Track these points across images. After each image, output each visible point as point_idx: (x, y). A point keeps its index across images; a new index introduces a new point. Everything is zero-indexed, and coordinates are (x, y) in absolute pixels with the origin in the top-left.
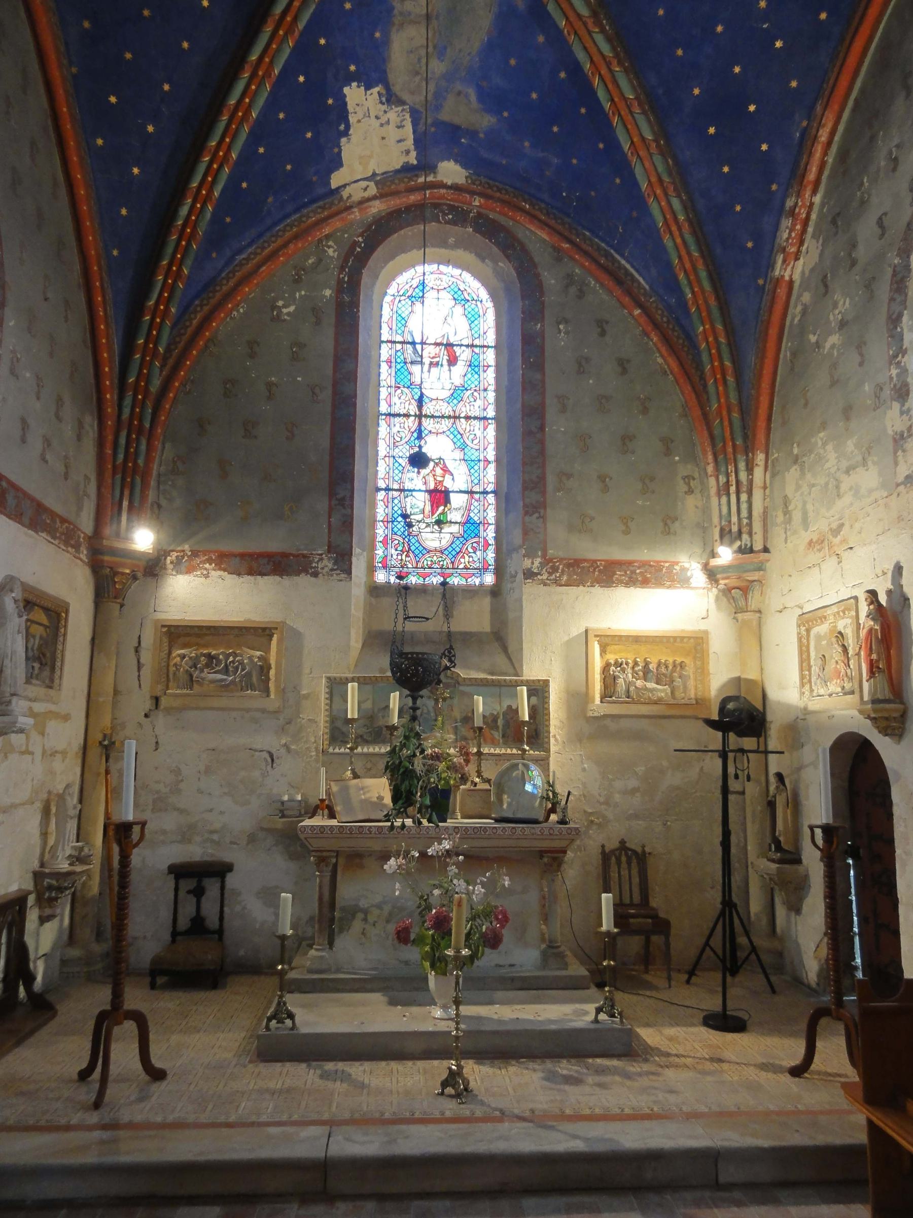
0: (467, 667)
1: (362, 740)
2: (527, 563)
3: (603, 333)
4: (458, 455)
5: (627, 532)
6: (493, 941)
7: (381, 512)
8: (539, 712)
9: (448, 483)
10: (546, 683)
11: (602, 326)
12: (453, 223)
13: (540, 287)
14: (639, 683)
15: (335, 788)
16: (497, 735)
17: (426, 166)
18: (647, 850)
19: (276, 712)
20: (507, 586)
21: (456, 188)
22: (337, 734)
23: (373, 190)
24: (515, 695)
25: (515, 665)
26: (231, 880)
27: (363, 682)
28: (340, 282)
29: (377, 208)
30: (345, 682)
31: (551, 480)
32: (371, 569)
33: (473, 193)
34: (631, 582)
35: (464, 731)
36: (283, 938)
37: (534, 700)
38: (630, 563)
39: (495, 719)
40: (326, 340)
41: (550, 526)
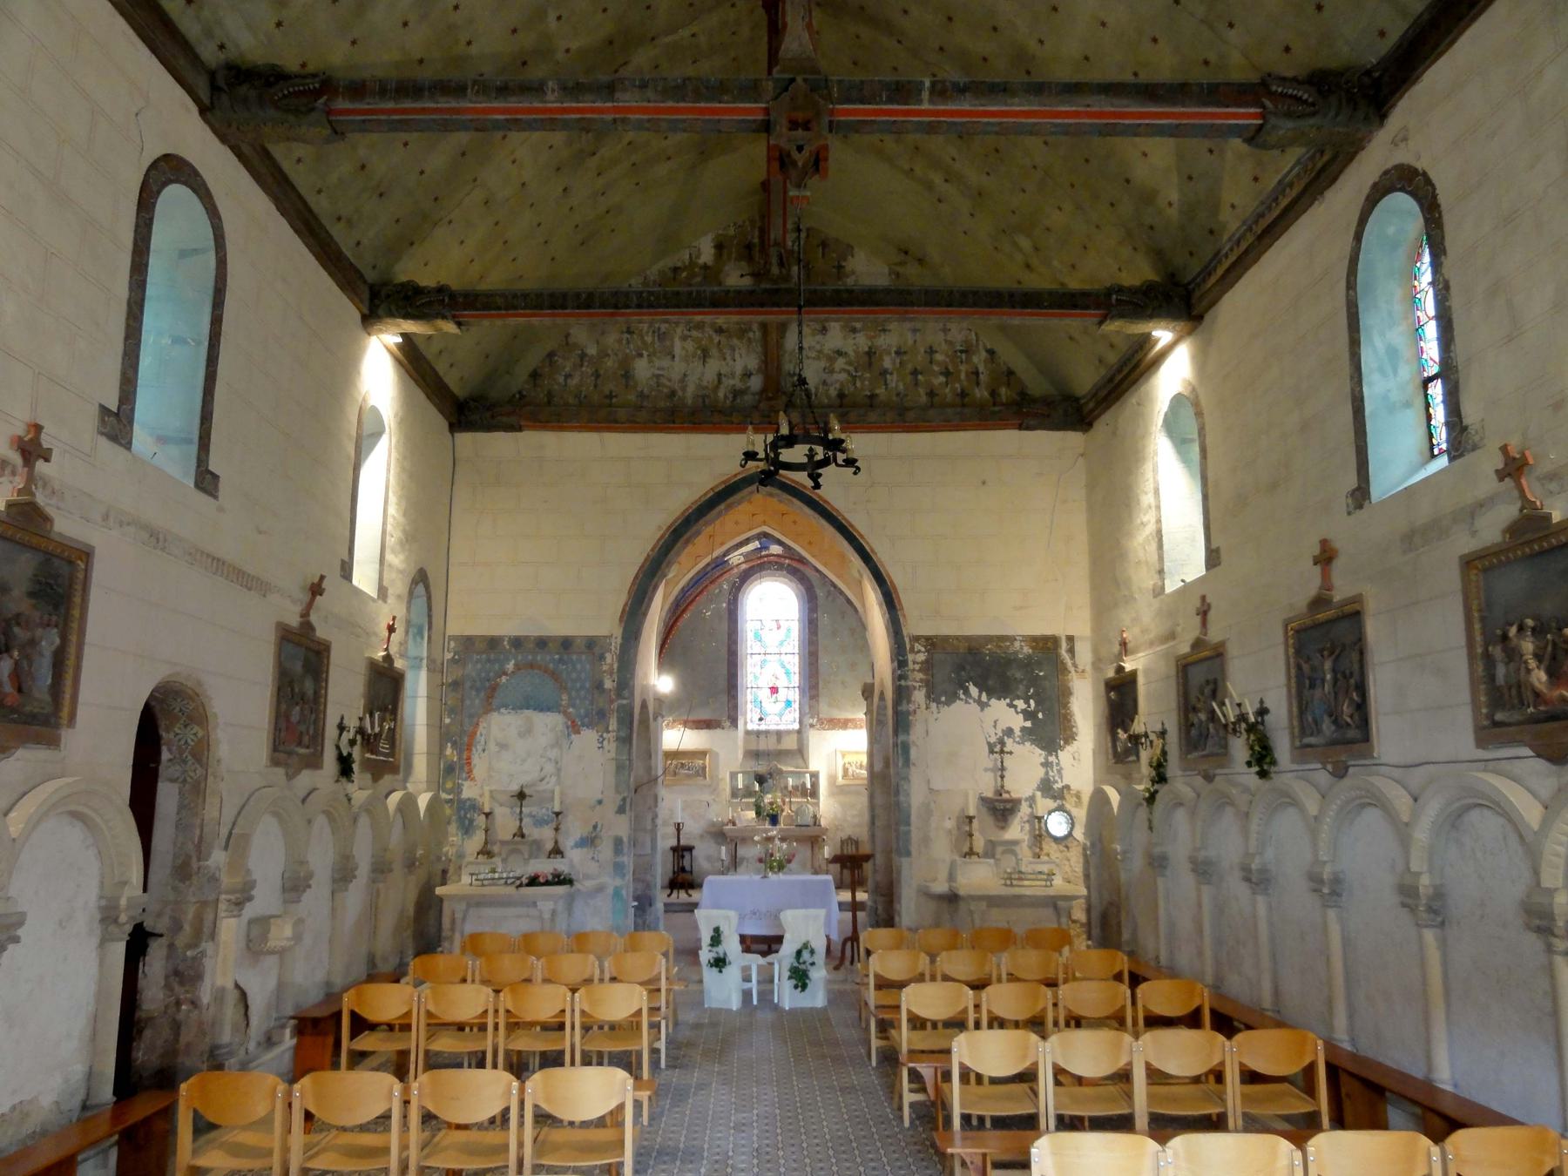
0: (786, 765)
3: (843, 617)
4: (783, 671)
6: (789, 861)
7: (749, 697)
8: (815, 785)
9: (778, 684)
10: (818, 772)
12: (777, 570)
14: (858, 771)
16: (799, 793)
17: (764, 548)
19: (710, 786)
21: (778, 556)
22: (735, 793)
23: (742, 559)
26: (694, 852)
27: (743, 773)
29: (744, 566)
30: (737, 773)
32: (746, 723)
33: (785, 558)
34: (855, 727)
35: (785, 792)
36: (723, 860)
38: (854, 720)
40: (725, 626)
41: (821, 705)
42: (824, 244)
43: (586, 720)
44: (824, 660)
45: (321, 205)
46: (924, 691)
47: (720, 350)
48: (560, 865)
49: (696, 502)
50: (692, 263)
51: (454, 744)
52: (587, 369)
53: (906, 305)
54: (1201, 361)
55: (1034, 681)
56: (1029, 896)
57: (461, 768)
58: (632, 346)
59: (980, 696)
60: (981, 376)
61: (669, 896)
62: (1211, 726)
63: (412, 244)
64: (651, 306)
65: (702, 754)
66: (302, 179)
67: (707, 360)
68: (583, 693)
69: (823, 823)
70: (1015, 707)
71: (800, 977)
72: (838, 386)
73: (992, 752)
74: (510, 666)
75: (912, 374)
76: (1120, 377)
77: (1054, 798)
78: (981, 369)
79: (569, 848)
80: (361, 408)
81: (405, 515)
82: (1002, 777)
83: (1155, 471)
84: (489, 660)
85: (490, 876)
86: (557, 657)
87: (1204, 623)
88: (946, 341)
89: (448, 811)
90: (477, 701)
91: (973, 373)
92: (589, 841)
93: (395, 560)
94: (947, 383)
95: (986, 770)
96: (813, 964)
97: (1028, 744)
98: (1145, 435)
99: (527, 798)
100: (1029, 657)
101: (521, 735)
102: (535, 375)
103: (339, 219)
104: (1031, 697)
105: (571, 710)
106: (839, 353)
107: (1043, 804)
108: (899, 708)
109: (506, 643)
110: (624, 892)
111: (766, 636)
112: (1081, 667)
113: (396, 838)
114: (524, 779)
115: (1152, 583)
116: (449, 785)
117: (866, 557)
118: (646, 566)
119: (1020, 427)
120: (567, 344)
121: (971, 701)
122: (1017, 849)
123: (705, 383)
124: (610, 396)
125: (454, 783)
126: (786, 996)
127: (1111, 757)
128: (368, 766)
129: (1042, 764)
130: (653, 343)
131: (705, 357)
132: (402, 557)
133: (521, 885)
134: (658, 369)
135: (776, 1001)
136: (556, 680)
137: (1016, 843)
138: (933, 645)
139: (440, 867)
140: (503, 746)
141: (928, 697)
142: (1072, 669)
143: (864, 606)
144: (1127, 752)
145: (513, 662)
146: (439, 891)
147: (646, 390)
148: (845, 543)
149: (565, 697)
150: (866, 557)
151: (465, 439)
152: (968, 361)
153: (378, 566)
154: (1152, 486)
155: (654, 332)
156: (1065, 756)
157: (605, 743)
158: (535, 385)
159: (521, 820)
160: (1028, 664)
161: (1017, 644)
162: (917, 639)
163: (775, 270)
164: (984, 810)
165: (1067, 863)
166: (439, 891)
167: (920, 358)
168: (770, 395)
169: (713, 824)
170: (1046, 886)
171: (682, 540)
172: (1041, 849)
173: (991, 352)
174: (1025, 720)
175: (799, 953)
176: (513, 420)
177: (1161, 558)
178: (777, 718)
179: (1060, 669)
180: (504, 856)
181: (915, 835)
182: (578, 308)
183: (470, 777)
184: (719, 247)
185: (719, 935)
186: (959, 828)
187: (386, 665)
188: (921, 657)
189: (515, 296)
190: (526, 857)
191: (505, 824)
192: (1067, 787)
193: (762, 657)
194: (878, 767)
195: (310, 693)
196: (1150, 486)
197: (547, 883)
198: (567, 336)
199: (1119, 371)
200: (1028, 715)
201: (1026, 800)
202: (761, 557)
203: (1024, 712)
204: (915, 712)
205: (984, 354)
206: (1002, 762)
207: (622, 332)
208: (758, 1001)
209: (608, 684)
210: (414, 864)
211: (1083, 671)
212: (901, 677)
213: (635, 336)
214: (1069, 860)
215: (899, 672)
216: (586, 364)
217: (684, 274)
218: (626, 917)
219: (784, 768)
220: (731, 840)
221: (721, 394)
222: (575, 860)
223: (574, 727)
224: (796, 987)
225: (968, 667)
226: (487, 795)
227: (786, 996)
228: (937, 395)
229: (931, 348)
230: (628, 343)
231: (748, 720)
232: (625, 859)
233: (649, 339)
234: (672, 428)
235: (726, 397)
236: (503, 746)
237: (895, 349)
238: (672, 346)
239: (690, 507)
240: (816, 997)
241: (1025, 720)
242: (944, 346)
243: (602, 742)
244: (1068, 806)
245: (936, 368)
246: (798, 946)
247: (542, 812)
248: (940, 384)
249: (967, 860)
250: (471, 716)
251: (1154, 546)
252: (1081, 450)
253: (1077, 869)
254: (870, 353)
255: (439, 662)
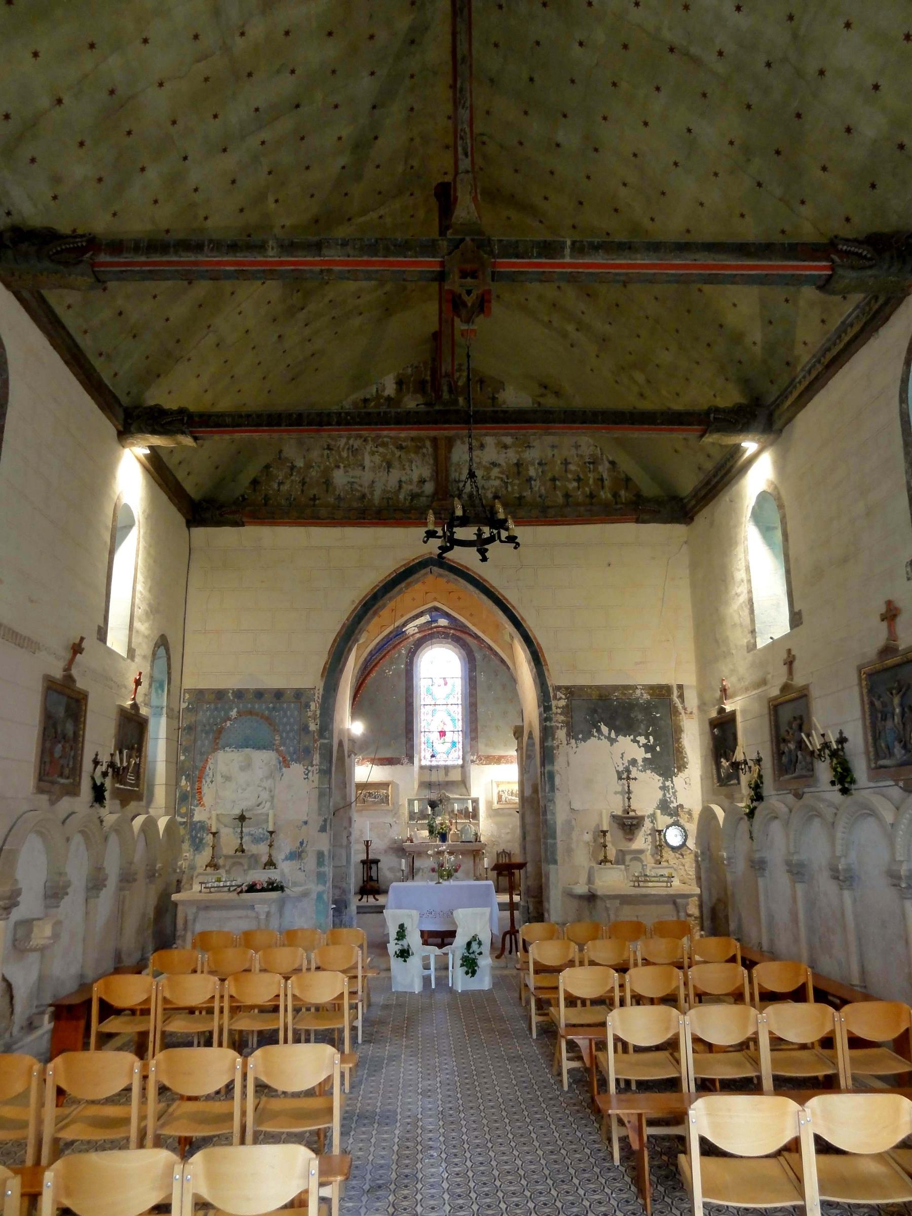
0: (452, 793)
1: (419, 819)
2: (472, 758)
5: (505, 745)
6: (456, 871)
7: (423, 739)
9: (446, 729)
11: (496, 673)
12: (444, 638)
13: (475, 659)
14: (510, 797)
15: (412, 833)
16: (463, 816)
17: (434, 621)
18: (512, 853)
20: (466, 765)
21: (445, 627)
22: (412, 816)
23: (417, 630)
24: (467, 803)
25: (469, 794)
27: (419, 800)
28: (407, 662)
29: (418, 636)
31: (479, 728)
32: (420, 760)
33: (451, 628)
34: (507, 762)
36: (403, 871)
37: (474, 804)
38: (507, 756)
39: (462, 810)
40: (403, 684)
41: (479, 744)
42: (481, 381)
43: (295, 756)
44: (481, 709)
45: (86, 343)
46: (565, 730)
47: (401, 462)
48: (273, 875)
49: (382, 581)
50: (378, 396)
51: (188, 777)
52: (296, 478)
53: (550, 422)
54: (781, 466)
55: (653, 721)
56: (654, 895)
57: (193, 797)
58: (331, 460)
59: (610, 734)
60: (606, 483)
61: (360, 900)
62: (799, 753)
63: (159, 376)
64: (348, 424)
65: (385, 785)
66: (70, 320)
67: (391, 470)
68: (291, 735)
69: (483, 839)
70: (638, 742)
71: (470, 965)
72: (493, 490)
73: (620, 778)
74: (234, 713)
75: (550, 480)
76: (716, 480)
77: (671, 815)
78: (605, 476)
79: (280, 861)
80: (116, 505)
81: (150, 591)
82: (629, 799)
83: (746, 552)
84: (216, 709)
85: (216, 884)
86: (271, 705)
87: (790, 672)
88: (577, 455)
89: (182, 831)
90: (207, 742)
91: (598, 479)
92: (296, 855)
93: (142, 627)
94: (579, 488)
95: (616, 793)
96: (480, 953)
97: (649, 772)
98: (737, 524)
99: (247, 820)
100: (648, 702)
101: (242, 769)
102: (255, 482)
103: (101, 355)
104: (650, 734)
105: (282, 748)
106: (494, 464)
107: (663, 820)
108: (546, 744)
109: (230, 694)
110: (325, 897)
111: (435, 689)
112: (689, 710)
113: (139, 855)
114: (244, 805)
115: (746, 641)
116: (183, 810)
117: (517, 623)
118: (343, 632)
119: (637, 521)
120: (280, 458)
121: (603, 738)
122: (642, 857)
123: (389, 488)
124: (314, 499)
125: (187, 809)
126: (459, 980)
127: (715, 781)
128: (117, 793)
129: (660, 788)
130: (348, 457)
131: (389, 467)
132: (146, 625)
133: (241, 892)
134: (352, 478)
135: (450, 985)
136: (270, 724)
137: (641, 852)
138: (572, 693)
139: (174, 878)
140: (228, 778)
141: (568, 735)
142: (682, 712)
143: (514, 664)
144: (729, 777)
145: (235, 710)
146: (175, 897)
147: (342, 494)
148: (500, 613)
149: (277, 737)
150: (517, 623)
151: (200, 533)
152: (596, 469)
153: (127, 632)
154: (743, 564)
155: (348, 449)
156: (678, 781)
157: (310, 774)
158: (255, 490)
159: (242, 838)
160: (647, 708)
161: (638, 692)
162: (558, 688)
163: (446, 396)
164: (615, 825)
165: (681, 867)
166: (175, 897)
167: (557, 468)
168: (440, 497)
169: (395, 842)
170: (667, 887)
171: (371, 612)
172: (662, 857)
173: (613, 463)
174: (646, 752)
175: (469, 945)
176: (237, 517)
177: (753, 621)
178: (445, 756)
179: (673, 711)
180: (227, 868)
181: (560, 846)
182: (291, 425)
183: (200, 803)
184: (400, 383)
185: (404, 931)
186: (595, 841)
187: (133, 712)
188: (563, 703)
189: (240, 416)
190: (246, 867)
191: (229, 840)
192: (681, 806)
193: (432, 708)
194: (528, 792)
195: (70, 734)
196: (741, 565)
197: (263, 890)
198: (281, 452)
199: (715, 476)
200: (648, 748)
201: (648, 817)
202: (432, 628)
203: (645, 746)
204: (558, 746)
205: (607, 465)
206: (629, 787)
207: (324, 449)
208: (436, 985)
209: (313, 727)
210: (154, 875)
211: (691, 713)
212: (546, 719)
213: (334, 452)
214: (684, 866)
215: (545, 715)
216: (295, 474)
217: (373, 404)
218: (327, 917)
219: (451, 796)
220: (410, 854)
221: (401, 497)
222: (285, 871)
223: (285, 762)
224: (467, 973)
225: (600, 710)
226: (214, 818)
227: (459, 980)
228: (571, 496)
229: (566, 460)
230: (328, 457)
231: (422, 758)
232: (326, 869)
233: (344, 454)
234: (364, 523)
235: (405, 499)
236: (228, 778)
237: (537, 461)
238: (363, 459)
239: (377, 585)
240: (483, 981)
241: (646, 752)
242: (576, 459)
243: (307, 774)
244: (682, 822)
245: (570, 476)
246: (467, 939)
247: (259, 831)
248: (574, 488)
249: (602, 866)
250: (202, 754)
251: (746, 612)
252: (685, 539)
253: (691, 873)
254: (518, 465)
255: (176, 709)
